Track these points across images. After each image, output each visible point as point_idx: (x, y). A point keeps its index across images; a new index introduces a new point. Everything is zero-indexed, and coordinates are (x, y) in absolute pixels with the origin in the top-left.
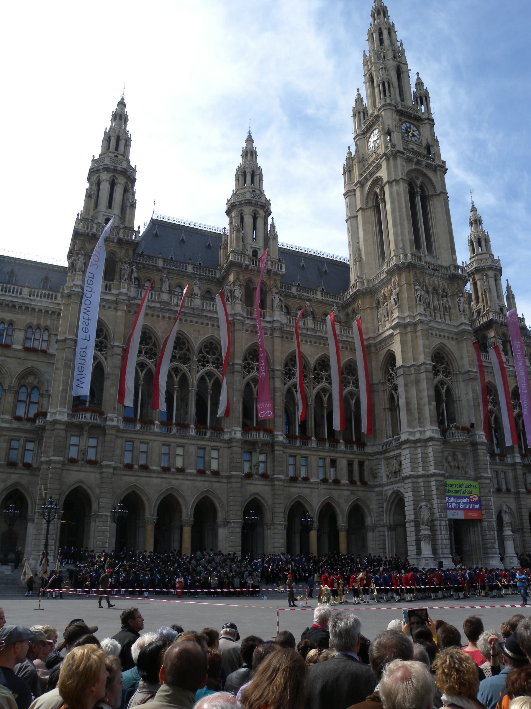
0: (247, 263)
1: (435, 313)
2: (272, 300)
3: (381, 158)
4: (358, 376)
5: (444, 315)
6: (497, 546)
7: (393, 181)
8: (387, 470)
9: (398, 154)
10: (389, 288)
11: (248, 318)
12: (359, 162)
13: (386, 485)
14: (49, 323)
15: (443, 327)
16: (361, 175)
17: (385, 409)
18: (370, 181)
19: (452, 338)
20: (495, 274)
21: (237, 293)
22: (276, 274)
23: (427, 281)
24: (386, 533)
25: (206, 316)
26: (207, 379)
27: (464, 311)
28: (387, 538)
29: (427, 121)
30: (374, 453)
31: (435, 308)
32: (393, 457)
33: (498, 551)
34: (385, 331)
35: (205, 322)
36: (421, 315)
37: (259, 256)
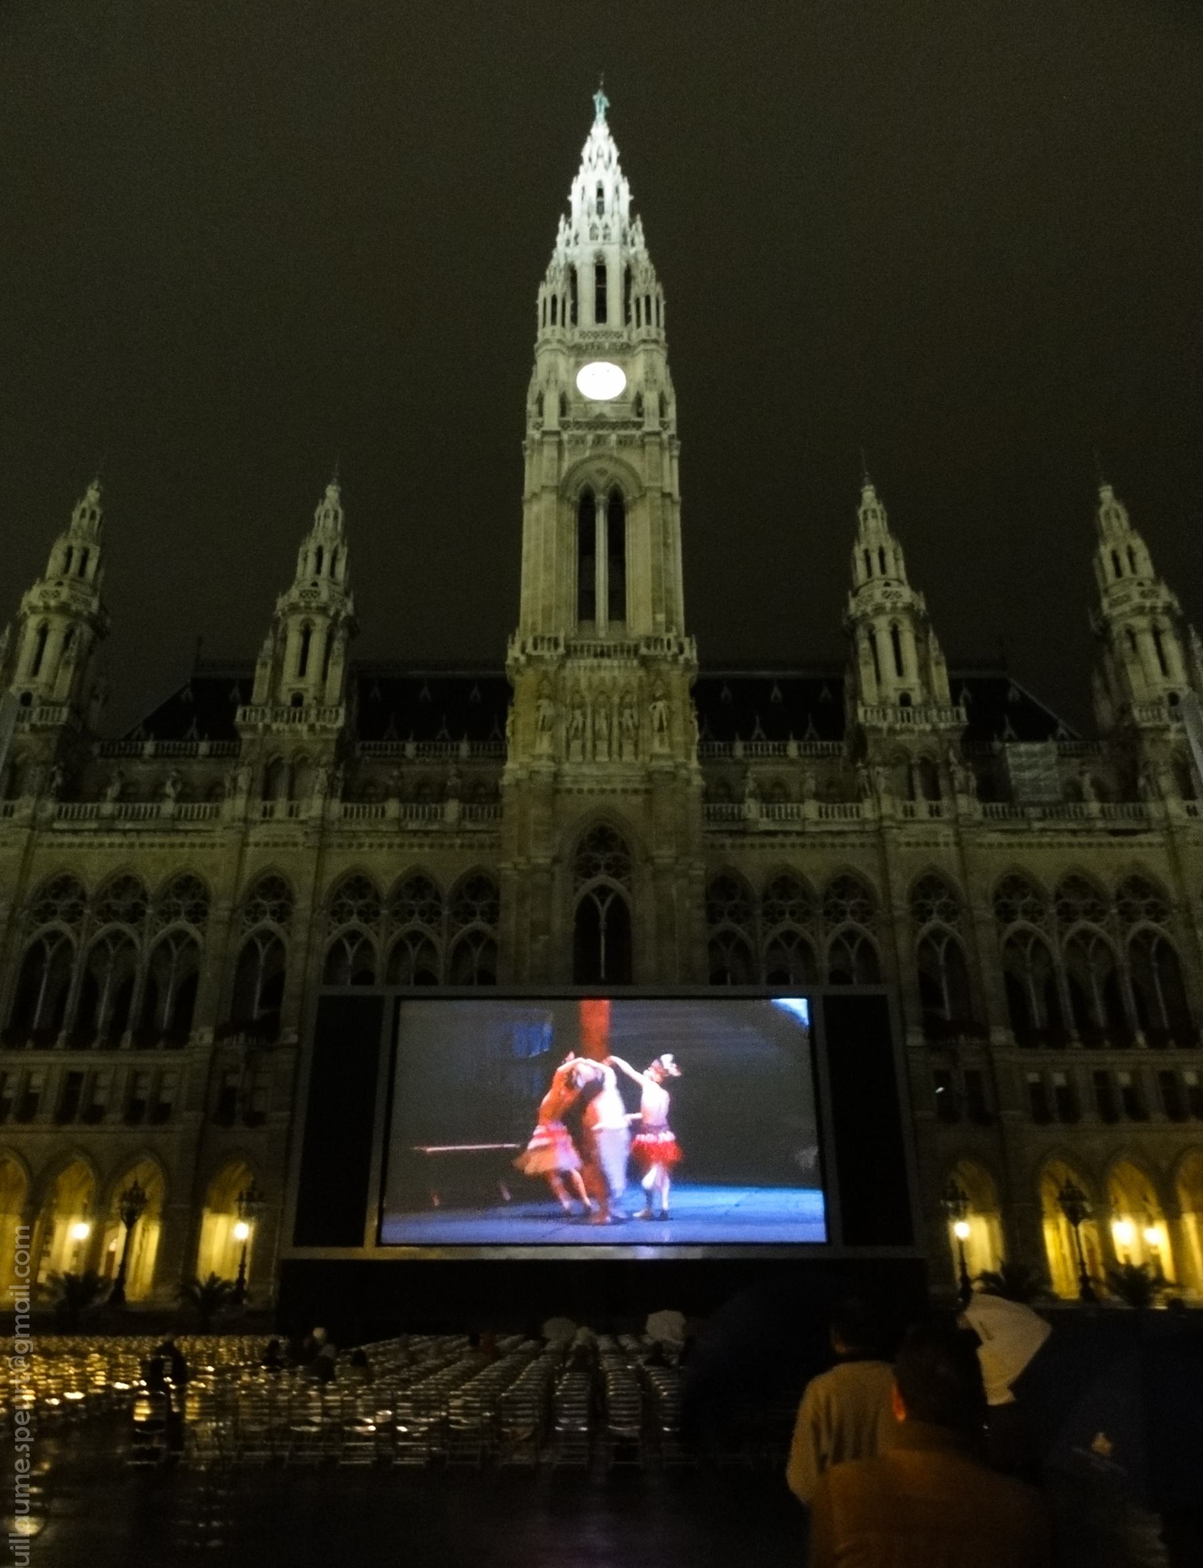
0: (267, 720)
1: (595, 746)
4: (497, 897)
5: (621, 747)
9: (546, 439)
11: (262, 822)
15: (612, 769)
20: (894, 619)
21: (243, 781)
22: (324, 729)
23: (583, 683)
25: (178, 831)
26: (173, 945)
27: (661, 729)
29: (642, 347)
31: (596, 736)
35: (178, 839)
36: (540, 757)
37: (305, 702)
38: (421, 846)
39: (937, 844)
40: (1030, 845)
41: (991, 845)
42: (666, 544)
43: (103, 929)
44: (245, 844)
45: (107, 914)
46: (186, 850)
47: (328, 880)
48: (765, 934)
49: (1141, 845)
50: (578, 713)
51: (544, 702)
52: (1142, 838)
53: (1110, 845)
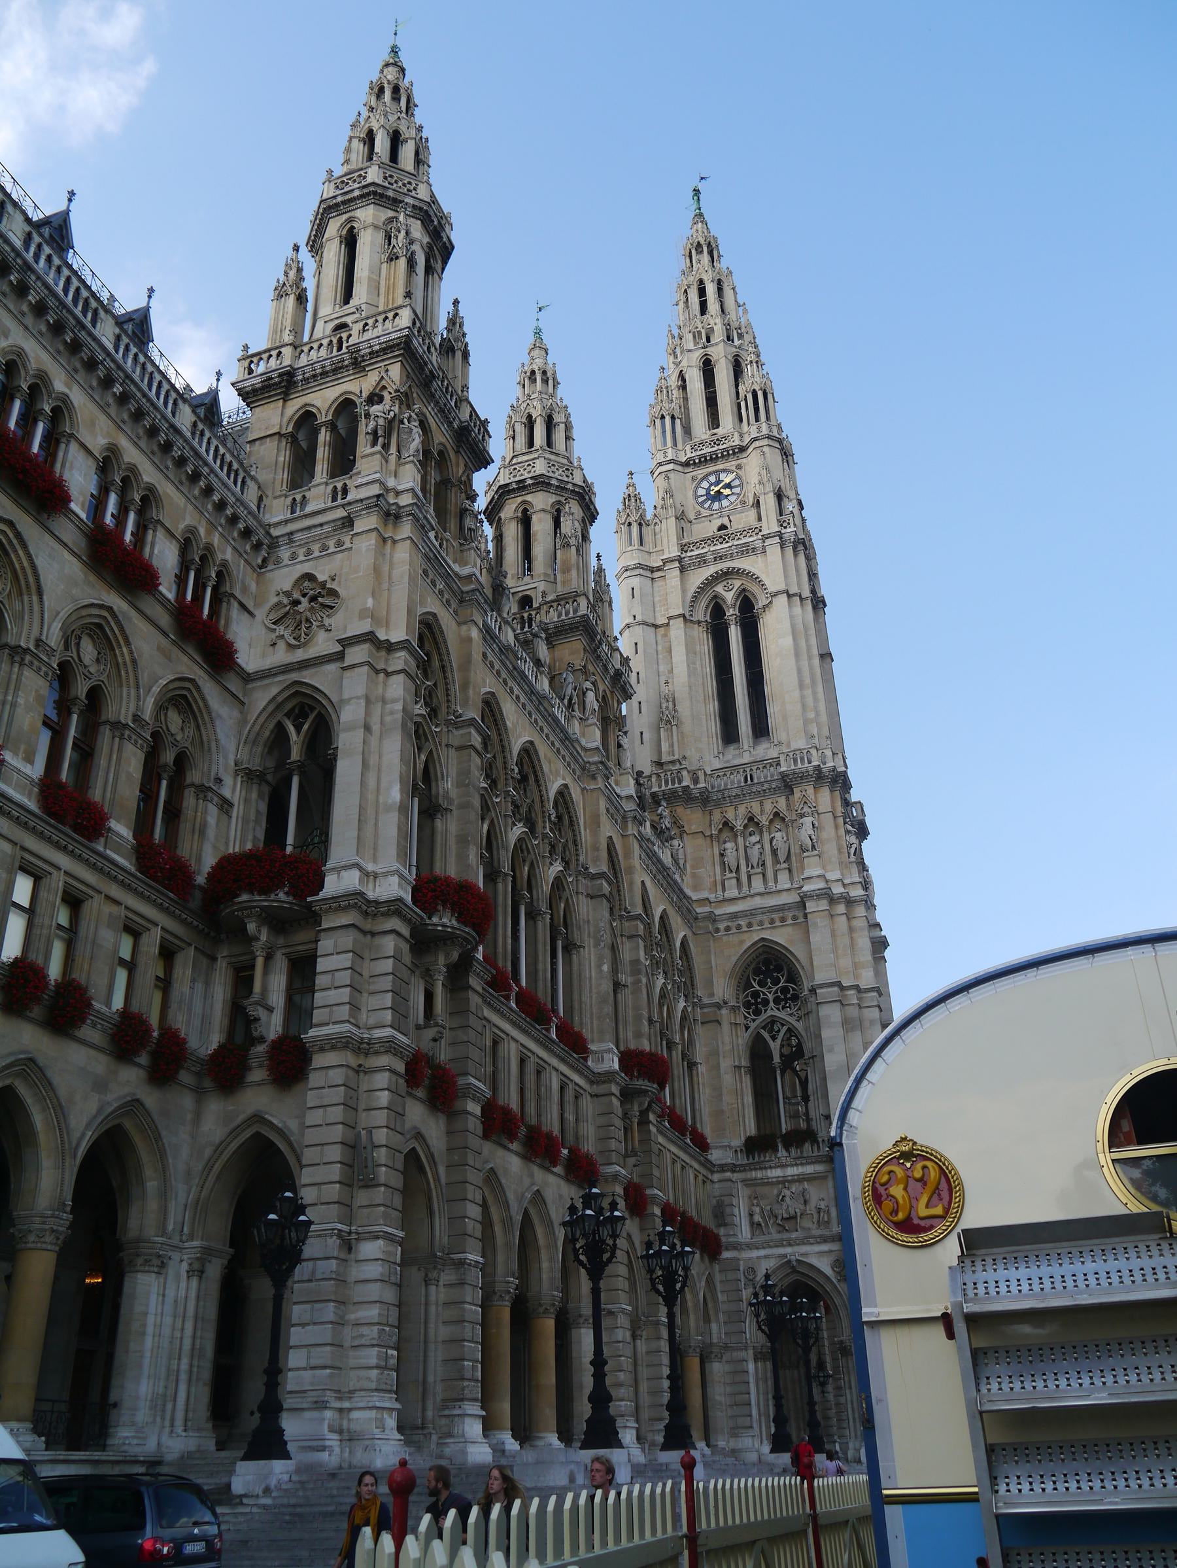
2: (620, 746)
3: (765, 537)
7: (796, 595)
8: (757, 1210)
10: (768, 806)
12: (677, 518)
13: (751, 1246)
14: (229, 555)
16: (683, 548)
17: (739, 1067)
18: (711, 570)
24: (751, 1366)
28: (752, 1380)
30: (721, 1166)
32: (783, 1182)
34: (752, 896)
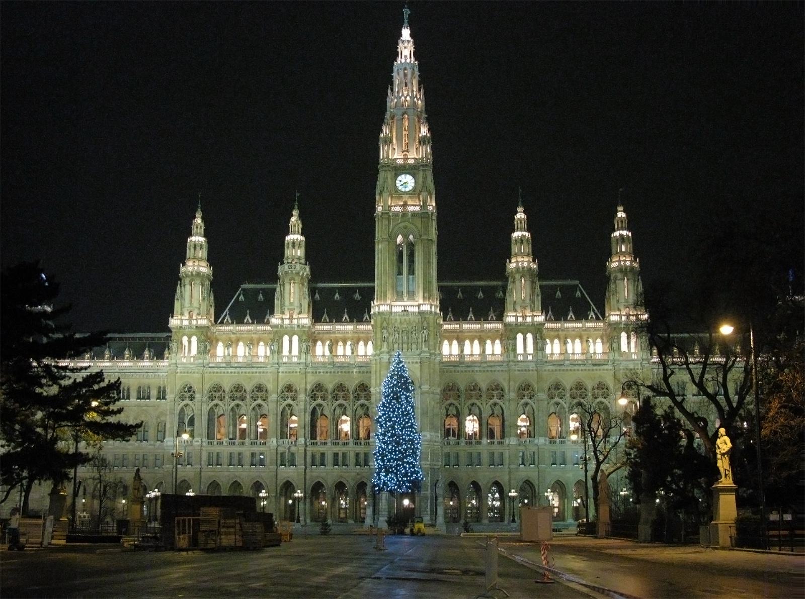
6: (429, 510)
19: (417, 363)
27: (425, 341)
33: (429, 513)
35: (254, 370)
38: (341, 372)
39: (529, 370)
40: (563, 370)
41: (549, 370)
42: (429, 262)
43: (233, 404)
44: (278, 373)
45: (233, 398)
46: (258, 374)
47: (309, 387)
48: (465, 404)
49: (604, 370)
50: (396, 332)
51: (385, 331)
52: (605, 367)
53: (593, 370)
